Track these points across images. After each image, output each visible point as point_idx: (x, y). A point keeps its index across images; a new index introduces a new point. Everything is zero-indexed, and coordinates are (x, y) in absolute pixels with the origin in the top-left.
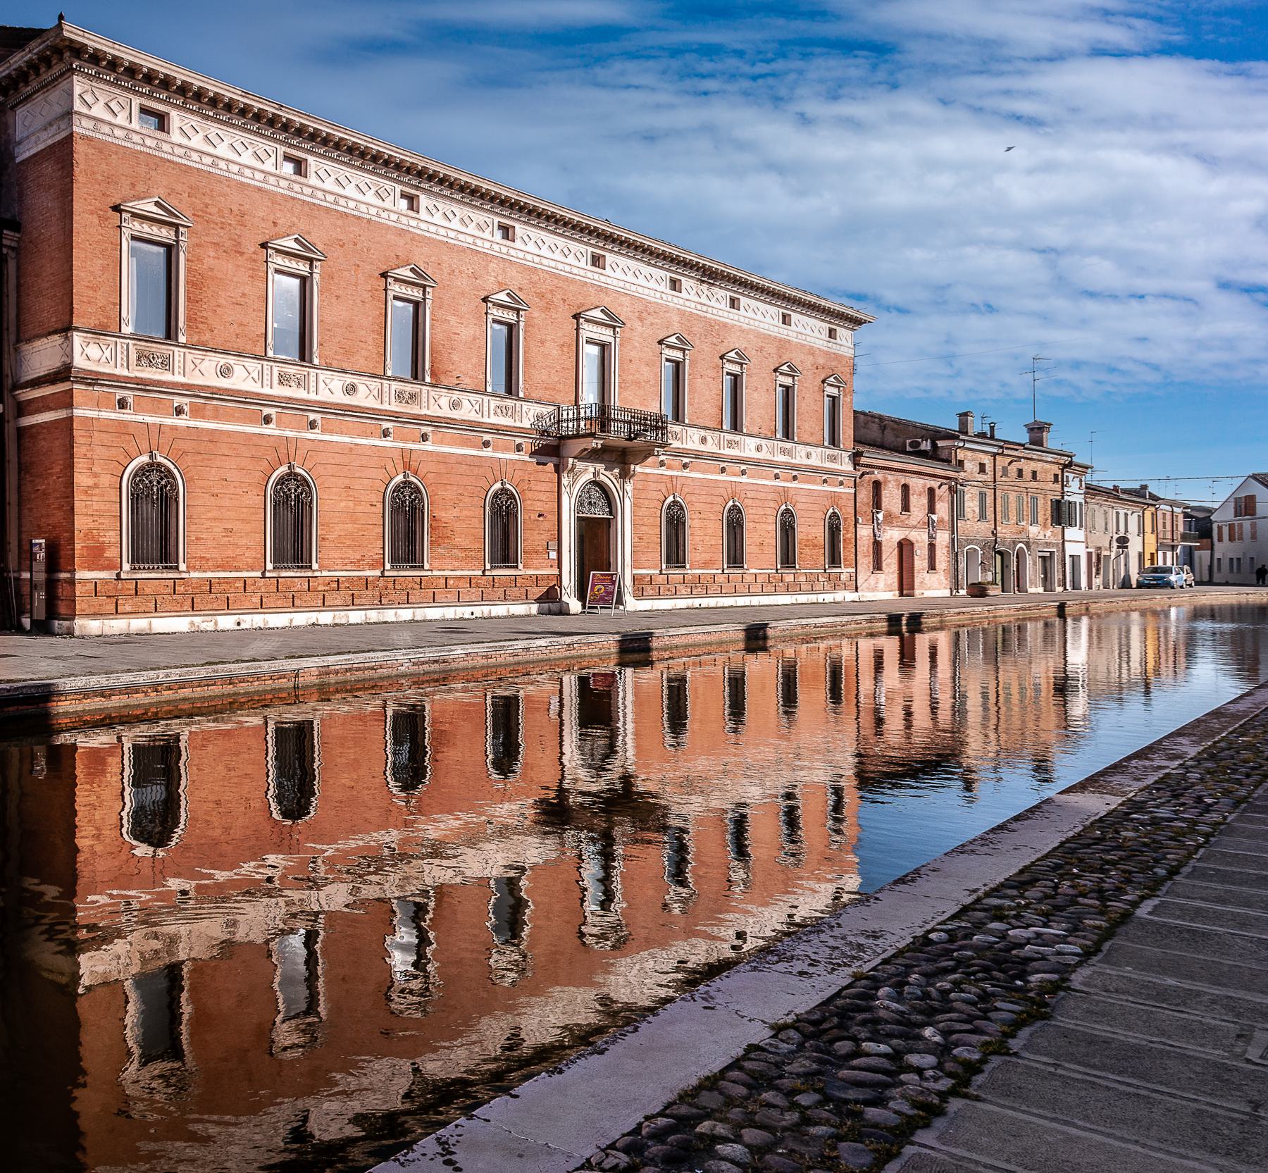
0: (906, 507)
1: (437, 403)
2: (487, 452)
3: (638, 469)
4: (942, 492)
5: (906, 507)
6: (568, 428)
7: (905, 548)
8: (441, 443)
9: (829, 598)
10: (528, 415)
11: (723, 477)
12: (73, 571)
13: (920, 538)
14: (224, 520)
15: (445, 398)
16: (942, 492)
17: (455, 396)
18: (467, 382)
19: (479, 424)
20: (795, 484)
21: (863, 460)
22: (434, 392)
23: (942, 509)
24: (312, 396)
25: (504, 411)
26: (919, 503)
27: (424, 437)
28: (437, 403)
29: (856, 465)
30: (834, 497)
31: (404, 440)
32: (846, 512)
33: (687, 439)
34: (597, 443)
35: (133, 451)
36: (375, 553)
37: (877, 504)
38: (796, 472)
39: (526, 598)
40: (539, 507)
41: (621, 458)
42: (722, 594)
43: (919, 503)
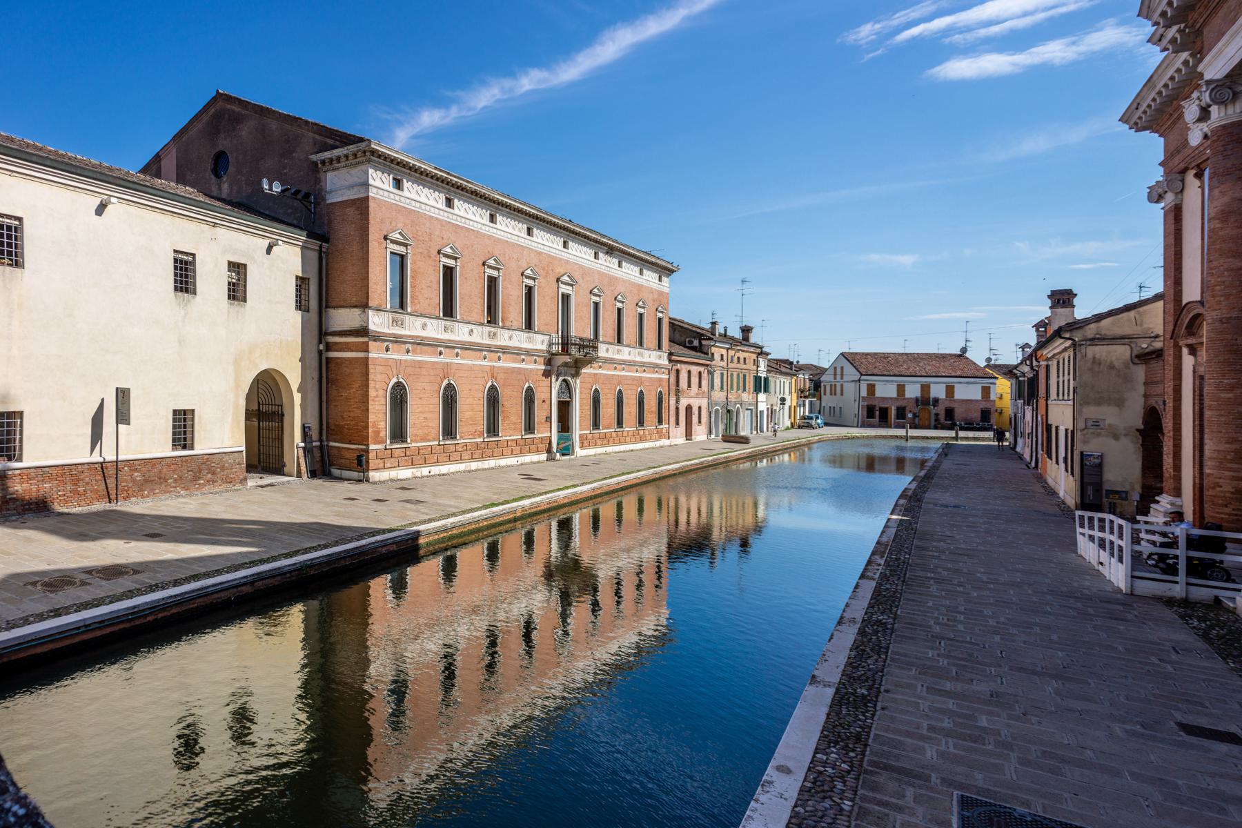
0: (689, 386)
1: (504, 338)
2: (523, 365)
3: (583, 370)
4: (705, 375)
5: (689, 386)
6: (554, 349)
7: (689, 409)
8: (505, 361)
9: (658, 444)
10: (539, 342)
11: (615, 373)
12: (367, 445)
13: (695, 403)
14: (423, 413)
15: (506, 333)
16: (705, 375)
17: (511, 332)
18: (515, 324)
19: (520, 349)
20: (644, 375)
21: (674, 358)
22: (502, 331)
23: (705, 383)
24: (457, 338)
25: (529, 340)
26: (695, 380)
27: (499, 359)
28: (504, 338)
29: (670, 361)
30: (660, 380)
31: (491, 360)
32: (665, 392)
33: (603, 351)
34: (567, 359)
35: (390, 373)
36: (480, 428)
37: (678, 385)
38: (645, 366)
39: (538, 451)
40: (545, 396)
41: (577, 366)
42: (614, 444)
43: (695, 380)
